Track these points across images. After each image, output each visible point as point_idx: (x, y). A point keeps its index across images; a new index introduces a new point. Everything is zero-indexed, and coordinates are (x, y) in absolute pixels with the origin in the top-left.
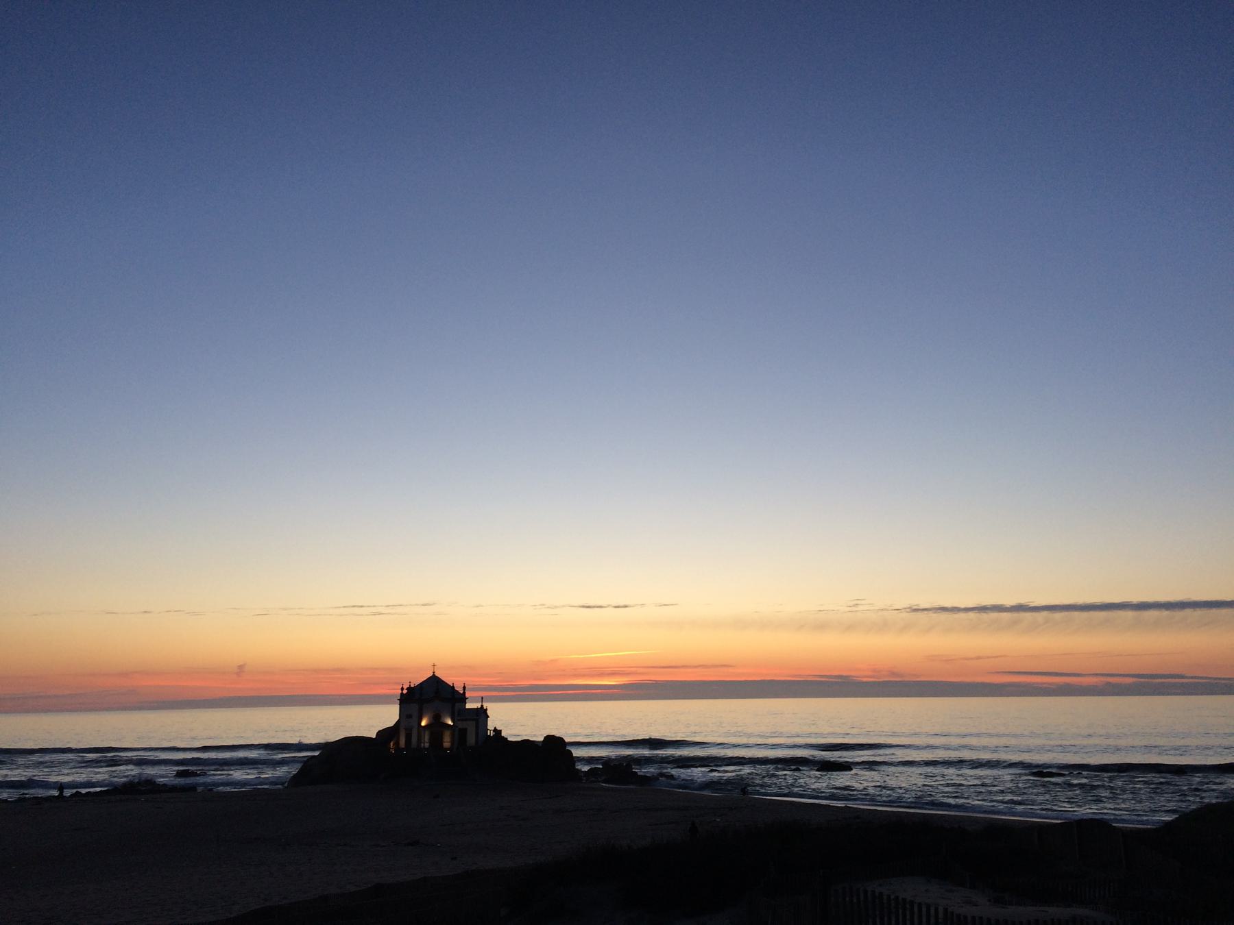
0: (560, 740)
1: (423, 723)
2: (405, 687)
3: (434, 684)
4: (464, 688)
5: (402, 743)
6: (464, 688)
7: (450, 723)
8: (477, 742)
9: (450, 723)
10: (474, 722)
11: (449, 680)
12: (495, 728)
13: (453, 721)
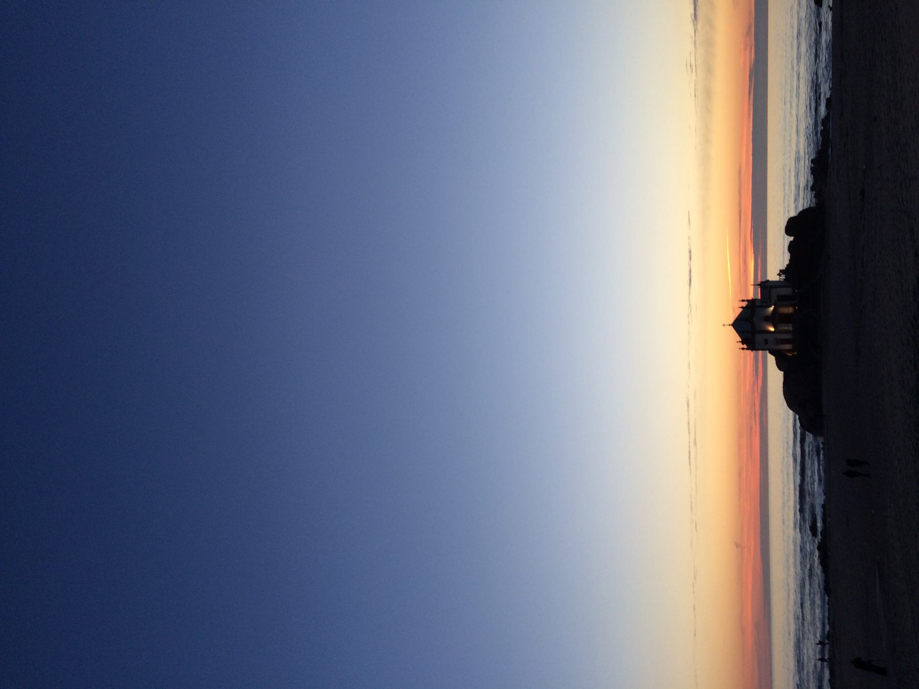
1: (772, 329)
2: (742, 346)
3: (738, 325)
4: (743, 301)
5: (788, 347)
6: (743, 301)
7: (772, 308)
9: (772, 308)
12: (778, 275)
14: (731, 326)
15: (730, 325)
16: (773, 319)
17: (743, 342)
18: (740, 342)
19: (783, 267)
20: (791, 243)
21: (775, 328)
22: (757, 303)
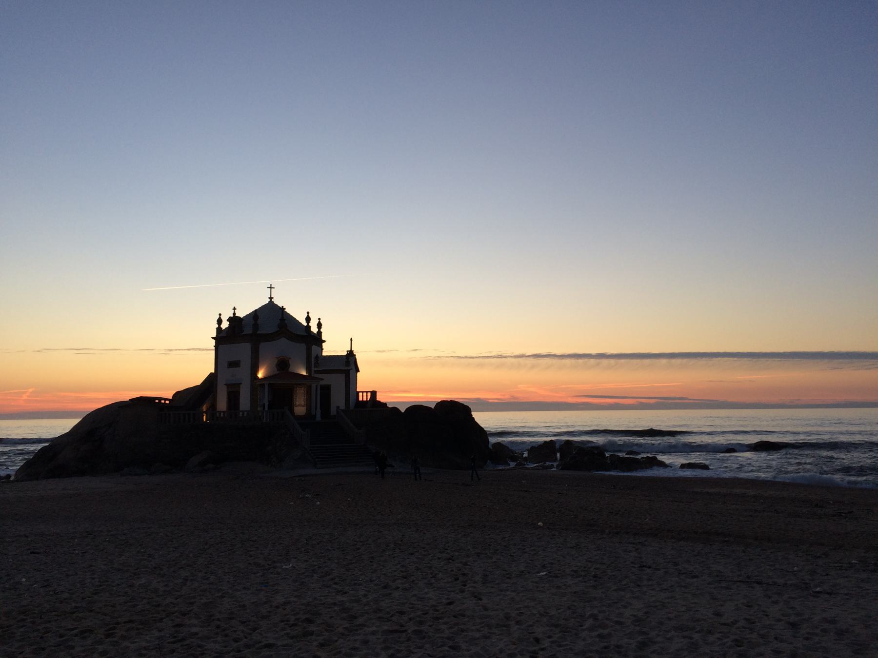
2: (225, 318)
4: (319, 325)
5: (222, 404)
6: (319, 325)
9: (304, 373)
10: (342, 377)
13: (308, 370)
14: (267, 301)
15: (271, 298)
17: (234, 320)
18: (234, 314)
19: (380, 398)
20: (432, 408)
21: (262, 379)
22: (314, 348)
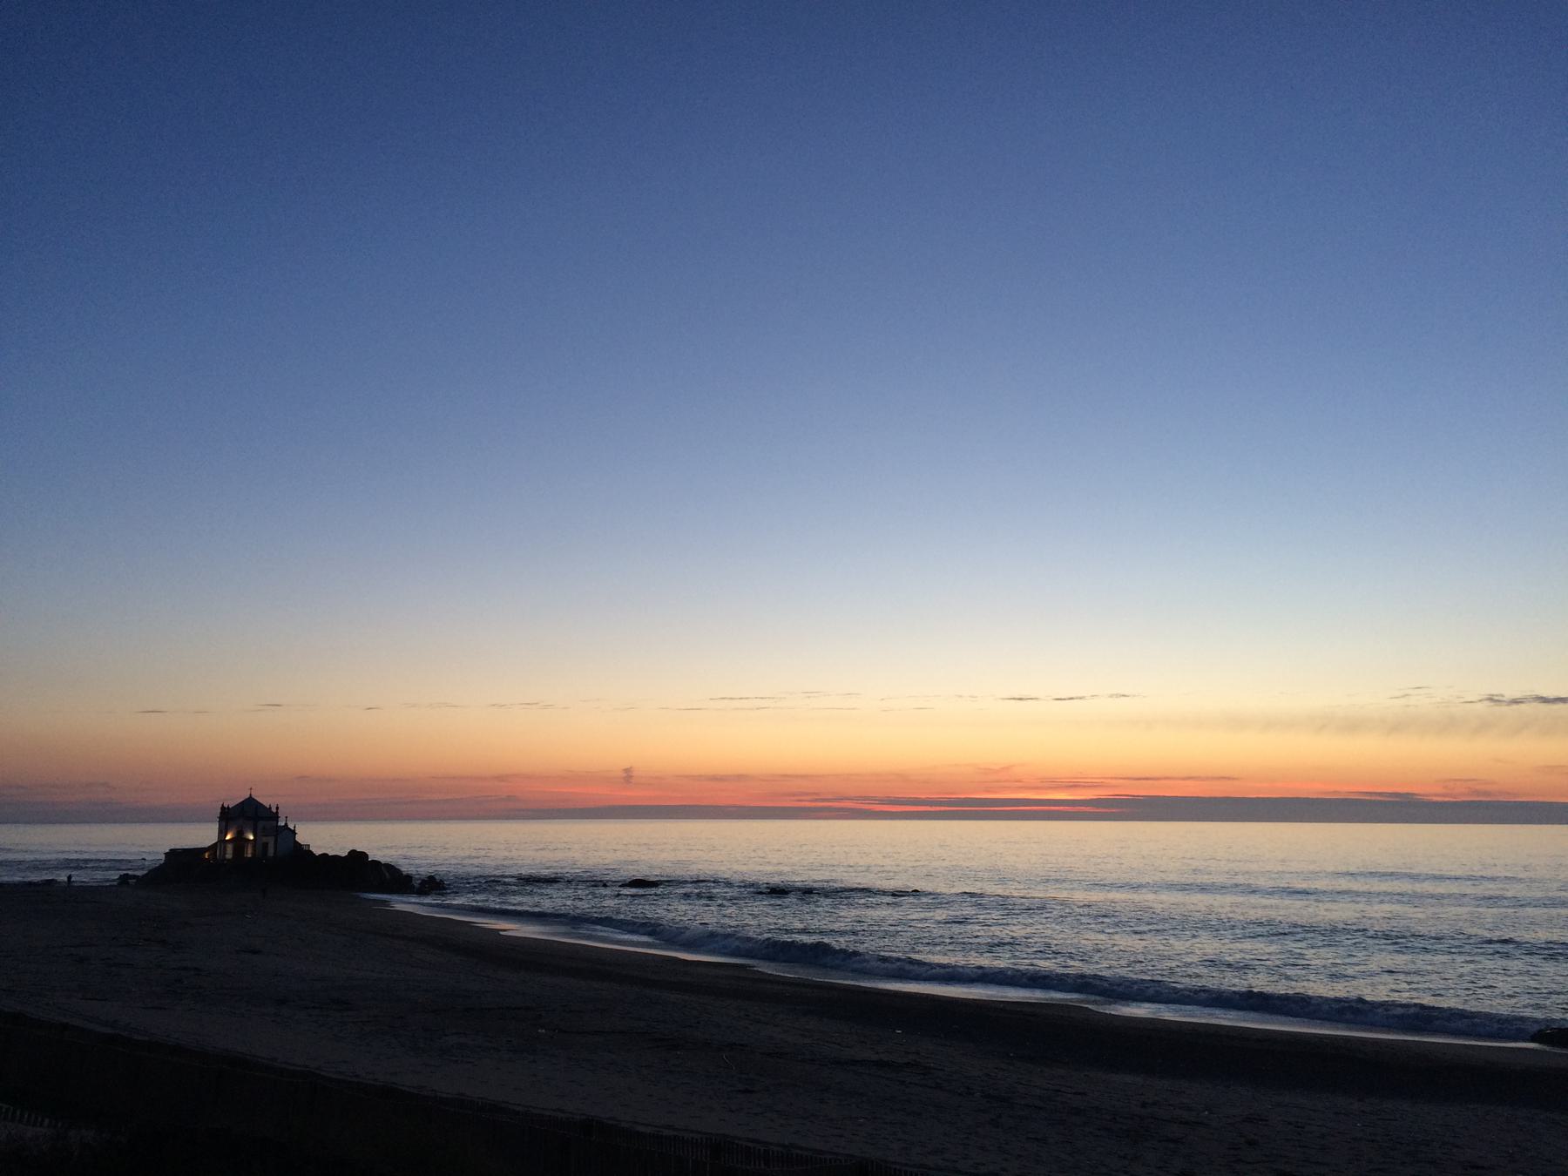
0: (364, 855)
1: (228, 837)
4: (277, 808)
6: (277, 808)
7: (251, 837)
8: (275, 853)
9: (251, 837)
11: (265, 802)
13: (254, 836)
14: (248, 796)
16: (239, 840)
